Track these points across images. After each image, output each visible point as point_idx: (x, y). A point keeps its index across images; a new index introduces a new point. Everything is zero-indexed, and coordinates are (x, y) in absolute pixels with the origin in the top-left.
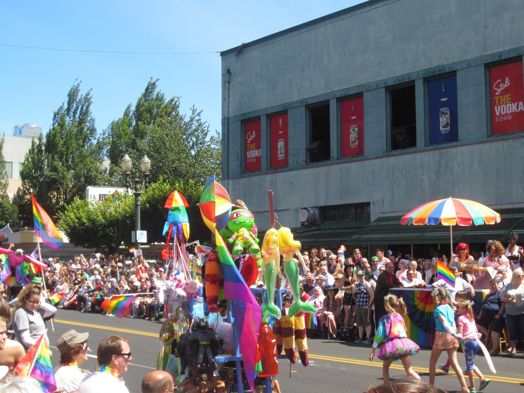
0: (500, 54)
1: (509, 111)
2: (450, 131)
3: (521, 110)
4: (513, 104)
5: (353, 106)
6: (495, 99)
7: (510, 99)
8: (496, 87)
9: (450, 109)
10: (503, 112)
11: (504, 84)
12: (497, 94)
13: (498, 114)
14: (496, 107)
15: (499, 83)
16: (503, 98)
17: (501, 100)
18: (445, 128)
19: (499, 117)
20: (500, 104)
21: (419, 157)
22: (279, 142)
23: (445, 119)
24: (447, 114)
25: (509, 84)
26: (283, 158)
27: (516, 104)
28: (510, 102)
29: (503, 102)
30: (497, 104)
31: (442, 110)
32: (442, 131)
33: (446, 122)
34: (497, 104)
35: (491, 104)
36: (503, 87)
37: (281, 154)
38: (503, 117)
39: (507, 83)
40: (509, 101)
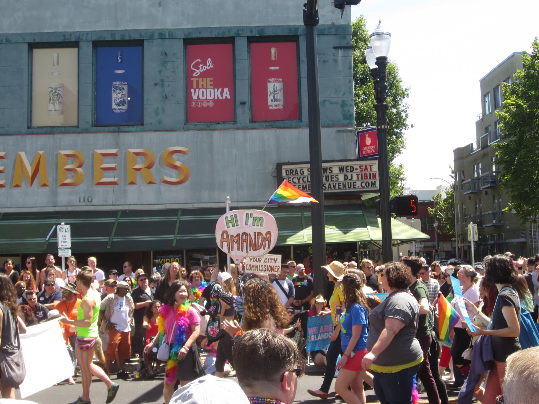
0: (262, 29)
1: (210, 96)
2: (127, 111)
3: (226, 97)
4: (216, 90)
5: (119, 57)
6: (192, 81)
7: (212, 83)
8: (193, 67)
9: (128, 84)
10: (203, 96)
11: (206, 66)
12: (194, 75)
13: (195, 97)
14: (192, 90)
15: (198, 63)
16: (203, 81)
17: (201, 83)
18: (120, 106)
19: (197, 102)
20: (198, 87)
21: (239, 134)
22: (270, 82)
23: (120, 96)
24: (123, 89)
25: (211, 66)
26: (282, 107)
27: (220, 90)
28: (212, 87)
29: (203, 85)
30: (195, 86)
31: (117, 83)
32: (115, 109)
33: (122, 99)
34: (195, 86)
35: (188, 86)
36: (203, 68)
37: (275, 100)
38: (202, 102)
39: (209, 65)
40: (211, 85)
